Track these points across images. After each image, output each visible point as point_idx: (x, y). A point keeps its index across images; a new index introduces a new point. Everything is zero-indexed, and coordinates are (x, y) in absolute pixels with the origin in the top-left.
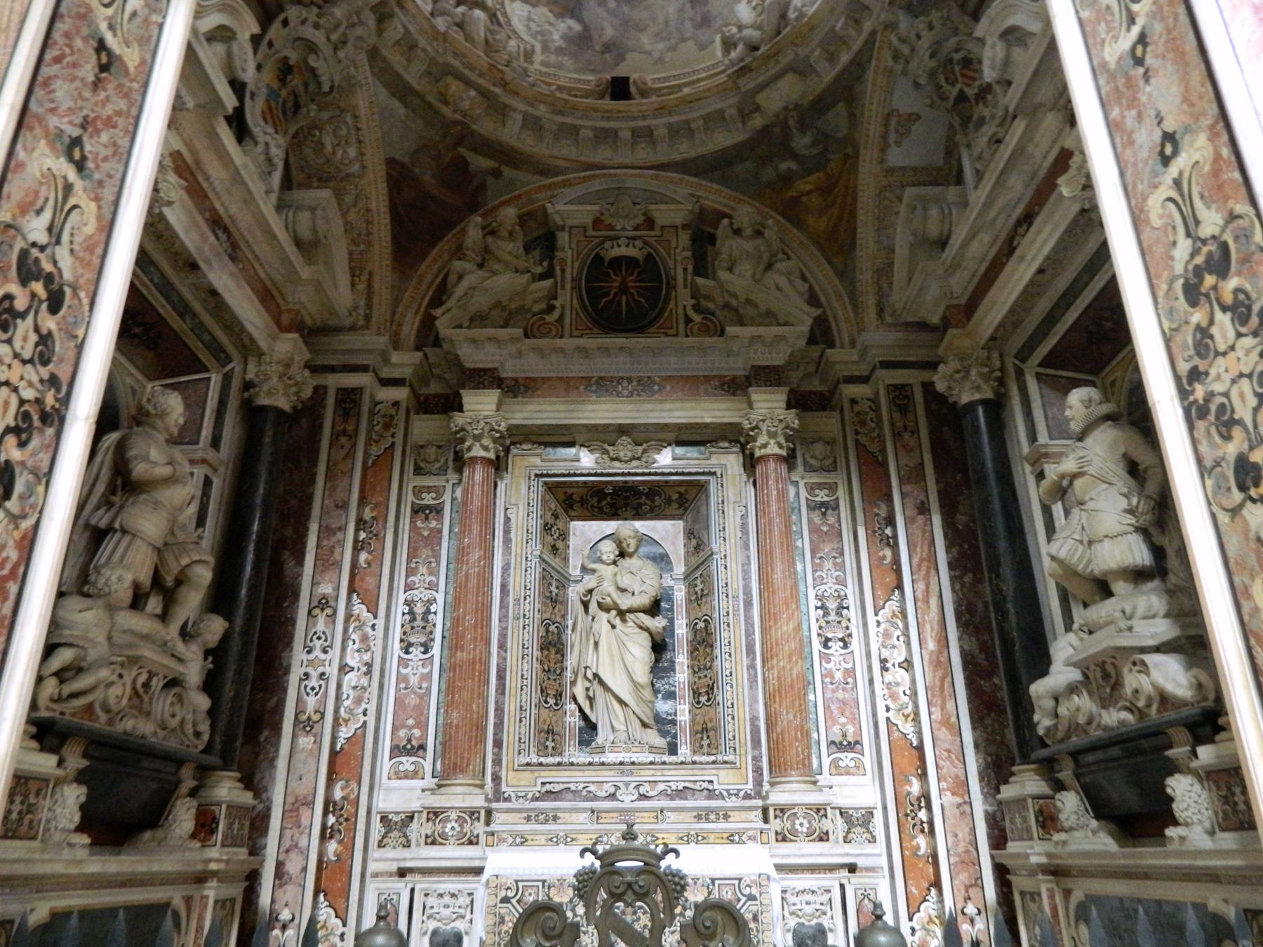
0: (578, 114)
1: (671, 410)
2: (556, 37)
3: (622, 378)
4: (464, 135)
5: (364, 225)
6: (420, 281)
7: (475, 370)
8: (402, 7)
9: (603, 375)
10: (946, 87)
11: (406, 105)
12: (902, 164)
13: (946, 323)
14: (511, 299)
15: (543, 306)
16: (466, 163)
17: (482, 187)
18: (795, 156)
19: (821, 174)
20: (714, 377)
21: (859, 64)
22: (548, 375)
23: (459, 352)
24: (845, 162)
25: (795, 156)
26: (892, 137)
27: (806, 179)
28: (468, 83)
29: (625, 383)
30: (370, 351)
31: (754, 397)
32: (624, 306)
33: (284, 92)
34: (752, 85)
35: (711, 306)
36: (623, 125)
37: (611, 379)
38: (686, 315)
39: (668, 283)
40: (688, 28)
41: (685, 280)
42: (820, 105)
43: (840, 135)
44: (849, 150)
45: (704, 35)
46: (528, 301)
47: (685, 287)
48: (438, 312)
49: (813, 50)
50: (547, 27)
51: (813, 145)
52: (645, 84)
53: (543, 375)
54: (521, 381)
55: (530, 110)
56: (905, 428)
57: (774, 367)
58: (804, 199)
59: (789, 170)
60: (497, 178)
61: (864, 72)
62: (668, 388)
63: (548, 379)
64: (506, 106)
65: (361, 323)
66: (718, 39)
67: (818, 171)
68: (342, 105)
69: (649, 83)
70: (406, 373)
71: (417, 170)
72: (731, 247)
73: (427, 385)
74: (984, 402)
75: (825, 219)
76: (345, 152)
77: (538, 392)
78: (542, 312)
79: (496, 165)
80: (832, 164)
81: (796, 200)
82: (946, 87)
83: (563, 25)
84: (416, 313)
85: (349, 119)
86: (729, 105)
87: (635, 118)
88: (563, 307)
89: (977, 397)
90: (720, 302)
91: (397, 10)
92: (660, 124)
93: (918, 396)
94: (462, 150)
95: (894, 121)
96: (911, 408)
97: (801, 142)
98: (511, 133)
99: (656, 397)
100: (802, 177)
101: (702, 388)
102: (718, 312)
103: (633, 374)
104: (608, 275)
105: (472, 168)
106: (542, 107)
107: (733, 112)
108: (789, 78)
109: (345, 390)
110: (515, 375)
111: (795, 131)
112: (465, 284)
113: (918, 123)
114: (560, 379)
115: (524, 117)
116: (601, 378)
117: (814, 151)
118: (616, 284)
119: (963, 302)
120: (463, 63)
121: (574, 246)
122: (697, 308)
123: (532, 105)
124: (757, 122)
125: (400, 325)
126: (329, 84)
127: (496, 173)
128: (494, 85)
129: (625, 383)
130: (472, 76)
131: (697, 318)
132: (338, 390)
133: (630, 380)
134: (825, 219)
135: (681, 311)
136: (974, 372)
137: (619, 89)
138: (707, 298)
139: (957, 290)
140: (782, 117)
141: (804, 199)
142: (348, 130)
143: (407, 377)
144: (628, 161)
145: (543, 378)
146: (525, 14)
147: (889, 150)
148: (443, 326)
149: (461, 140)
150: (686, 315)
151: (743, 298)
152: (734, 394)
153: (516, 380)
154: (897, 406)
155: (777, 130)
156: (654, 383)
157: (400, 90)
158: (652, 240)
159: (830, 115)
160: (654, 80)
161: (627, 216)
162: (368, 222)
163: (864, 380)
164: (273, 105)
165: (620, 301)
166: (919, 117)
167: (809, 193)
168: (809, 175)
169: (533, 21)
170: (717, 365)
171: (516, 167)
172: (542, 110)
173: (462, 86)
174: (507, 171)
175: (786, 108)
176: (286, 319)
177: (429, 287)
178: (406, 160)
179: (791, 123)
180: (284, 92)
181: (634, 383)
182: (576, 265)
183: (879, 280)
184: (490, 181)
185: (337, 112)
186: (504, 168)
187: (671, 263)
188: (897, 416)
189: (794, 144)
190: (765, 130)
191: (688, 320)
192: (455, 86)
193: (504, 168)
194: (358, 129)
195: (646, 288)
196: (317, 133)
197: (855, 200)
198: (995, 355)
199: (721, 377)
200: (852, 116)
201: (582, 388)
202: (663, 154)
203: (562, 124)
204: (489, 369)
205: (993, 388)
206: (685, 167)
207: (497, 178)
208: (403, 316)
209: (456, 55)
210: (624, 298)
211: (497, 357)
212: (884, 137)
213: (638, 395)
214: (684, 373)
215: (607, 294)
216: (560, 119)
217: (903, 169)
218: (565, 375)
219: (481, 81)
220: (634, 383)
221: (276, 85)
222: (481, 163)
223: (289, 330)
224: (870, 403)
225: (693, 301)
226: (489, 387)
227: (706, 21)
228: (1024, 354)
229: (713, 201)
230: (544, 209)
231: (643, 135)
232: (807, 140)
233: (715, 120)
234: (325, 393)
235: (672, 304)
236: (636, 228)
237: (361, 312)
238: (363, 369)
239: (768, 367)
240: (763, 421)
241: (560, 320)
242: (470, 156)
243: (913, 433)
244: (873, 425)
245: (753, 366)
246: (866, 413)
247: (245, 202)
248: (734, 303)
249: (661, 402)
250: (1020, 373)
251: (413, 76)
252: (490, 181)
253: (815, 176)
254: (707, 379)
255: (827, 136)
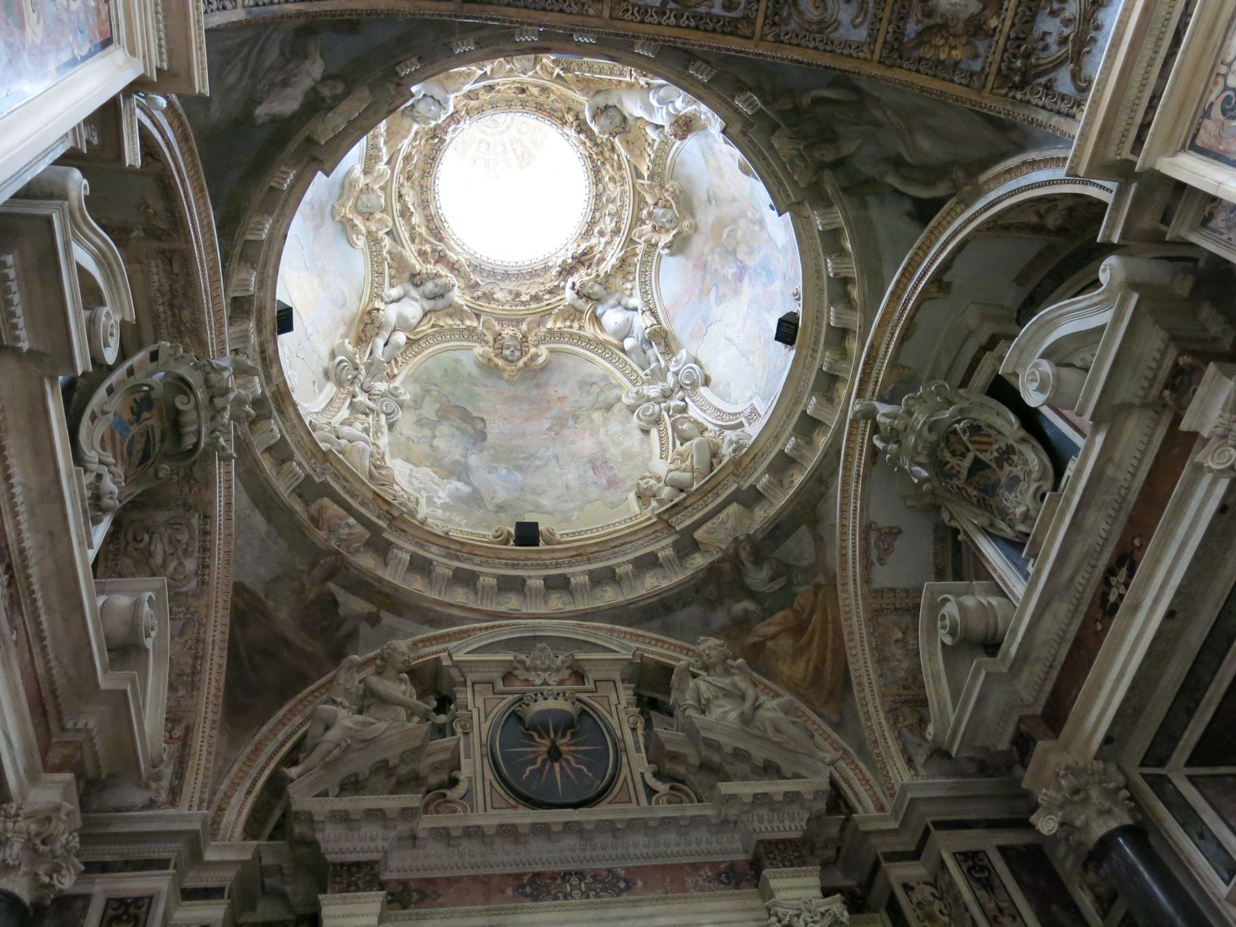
0: (477, 559)
1: (651, 916)
2: (442, 494)
3: (569, 873)
4: (338, 569)
5: (190, 661)
6: (257, 751)
7: (342, 864)
8: (281, 412)
9: (539, 869)
10: (953, 461)
11: (269, 519)
12: (890, 585)
13: (1023, 744)
14: (402, 760)
15: (444, 777)
16: (335, 603)
17: (353, 635)
18: (751, 594)
19: (787, 613)
20: (703, 864)
21: (821, 479)
22: (456, 873)
23: (319, 836)
24: (816, 594)
25: (751, 594)
26: (874, 554)
27: (768, 621)
28: (350, 510)
29: (574, 880)
30: (171, 835)
31: (774, 883)
32: (558, 776)
33: (134, 429)
34: (688, 522)
35: (681, 769)
36: (531, 573)
37: (553, 876)
38: (646, 786)
39: (615, 745)
40: (594, 492)
41: (636, 742)
42: (778, 531)
43: (805, 563)
44: (820, 579)
45: (613, 496)
46: (424, 765)
47: (638, 750)
48: (293, 772)
49: (759, 479)
50: (432, 485)
51: (772, 579)
52: (553, 535)
53: (448, 874)
54: (413, 886)
55: (420, 552)
56: (1000, 910)
57: (790, 841)
58: (770, 644)
59: (746, 611)
60: (373, 626)
61: (827, 488)
62: (640, 884)
63: (458, 879)
64: (390, 544)
65: (163, 797)
66: (632, 496)
67: (782, 609)
68: (190, 501)
69: (558, 537)
70: (226, 878)
71: (270, 603)
72: (698, 691)
73: (253, 908)
74: (1124, 830)
75: (802, 664)
76: (181, 564)
77: (440, 900)
78: (441, 786)
79: (374, 609)
80: (799, 600)
81: (759, 648)
82: (953, 461)
83: (448, 486)
84: (249, 792)
85: (195, 521)
86: (663, 547)
87: (546, 567)
88: (470, 780)
89: (1114, 824)
90: (694, 760)
91: (275, 413)
92: (579, 574)
93: (1000, 866)
94: (332, 586)
95: (873, 536)
96: (997, 882)
97: (758, 578)
98: (394, 575)
99: (623, 897)
100: (763, 619)
101: (690, 881)
102: (692, 777)
103: (586, 867)
104: (531, 738)
105: (341, 611)
106: (434, 549)
107: (669, 552)
108: (734, 508)
109: (122, 902)
110: (403, 876)
111: (748, 565)
112: (334, 734)
113: (900, 538)
114: (474, 878)
115: (411, 556)
116: (537, 875)
117: (776, 586)
118: (544, 749)
119: (1039, 710)
120: (344, 488)
121: (480, 703)
122: (657, 775)
123: (422, 547)
124: (699, 561)
125: (221, 809)
126: (194, 440)
127: (373, 620)
128: (378, 517)
129: (574, 880)
130: (355, 505)
131: (662, 787)
132: (108, 901)
133: (581, 875)
134: (802, 664)
135: (638, 779)
136: (1094, 793)
137: (527, 534)
138: (675, 757)
139: (1027, 697)
140: (731, 551)
141: (770, 644)
142: (191, 537)
143: (227, 885)
144: (542, 610)
145: (448, 879)
146: (408, 472)
147: (873, 569)
148: (301, 798)
149: (331, 575)
150: (646, 786)
151: (729, 750)
152: (737, 887)
153: (404, 883)
154: (979, 880)
155: (727, 566)
156: (618, 878)
157: (264, 499)
158: (583, 696)
159: (790, 543)
160: (562, 535)
161: (548, 669)
162: (196, 657)
163: (916, 855)
164: (118, 436)
165: (552, 768)
166: (900, 532)
167: (774, 637)
168: (772, 614)
169: (417, 478)
170: (704, 846)
171: (399, 614)
172: (433, 553)
173: (342, 512)
174: (387, 618)
175: (736, 540)
176: (55, 756)
177: (271, 758)
178: (259, 589)
179: (743, 555)
180: (134, 429)
181: (589, 880)
182: (485, 727)
183: (895, 723)
184: (364, 628)
185: (181, 511)
186: (383, 614)
187: (614, 723)
188: (982, 894)
189: (748, 581)
190: (712, 569)
191: (651, 792)
192: (333, 509)
193: (383, 614)
194: (206, 533)
195: (585, 753)
196: (146, 537)
197: (838, 633)
198: (1112, 768)
199: (714, 865)
200: (819, 541)
201: (509, 891)
202: (583, 604)
203: (458, 568)
204: (366, 863)
205: (1130, 810)
206: (616, 615)
207: (373, 626)
208: (227, 796)
209: (337, 476)
210: (557, 766)
211: (380, 844)
212: (865, 552)
213: (597, 896)
214: (660, 862)
215: (534, 761)
216: (456, 564)
217: (893, 590)
218: (482, 872)
219: (363, 510)
220: (589, 880)
221: (127, 416)
222: (353, 605)
223: (59, 769)
224: (929, 889)
225: (653, 767)
226: (369, 886)
227: (612, 483)
228: (1157, 755)
229: (652, 652)
230: (438, 660)
231: (559, 584)
232: (765, 573)
233: (648, 563)
234: (85, 909)
235: (625, 771)
236: (561, 683)
237: (165, 783)
238: (162, 864)
239: (782, 841)
240: (798, 916)
241: (468, 795)
242: (342, 596)
243: (1014, 918)
244: (946, 919)
245: (761, 842)
246: (930, 903)
247: (51, 535)
248: (716, 758)
249: (635, 903)
250: (1159, 784)
251: (283, 489)
252: (364, 628)
253: (779, 616)
254: (695, 867)
255: (789, 567)
